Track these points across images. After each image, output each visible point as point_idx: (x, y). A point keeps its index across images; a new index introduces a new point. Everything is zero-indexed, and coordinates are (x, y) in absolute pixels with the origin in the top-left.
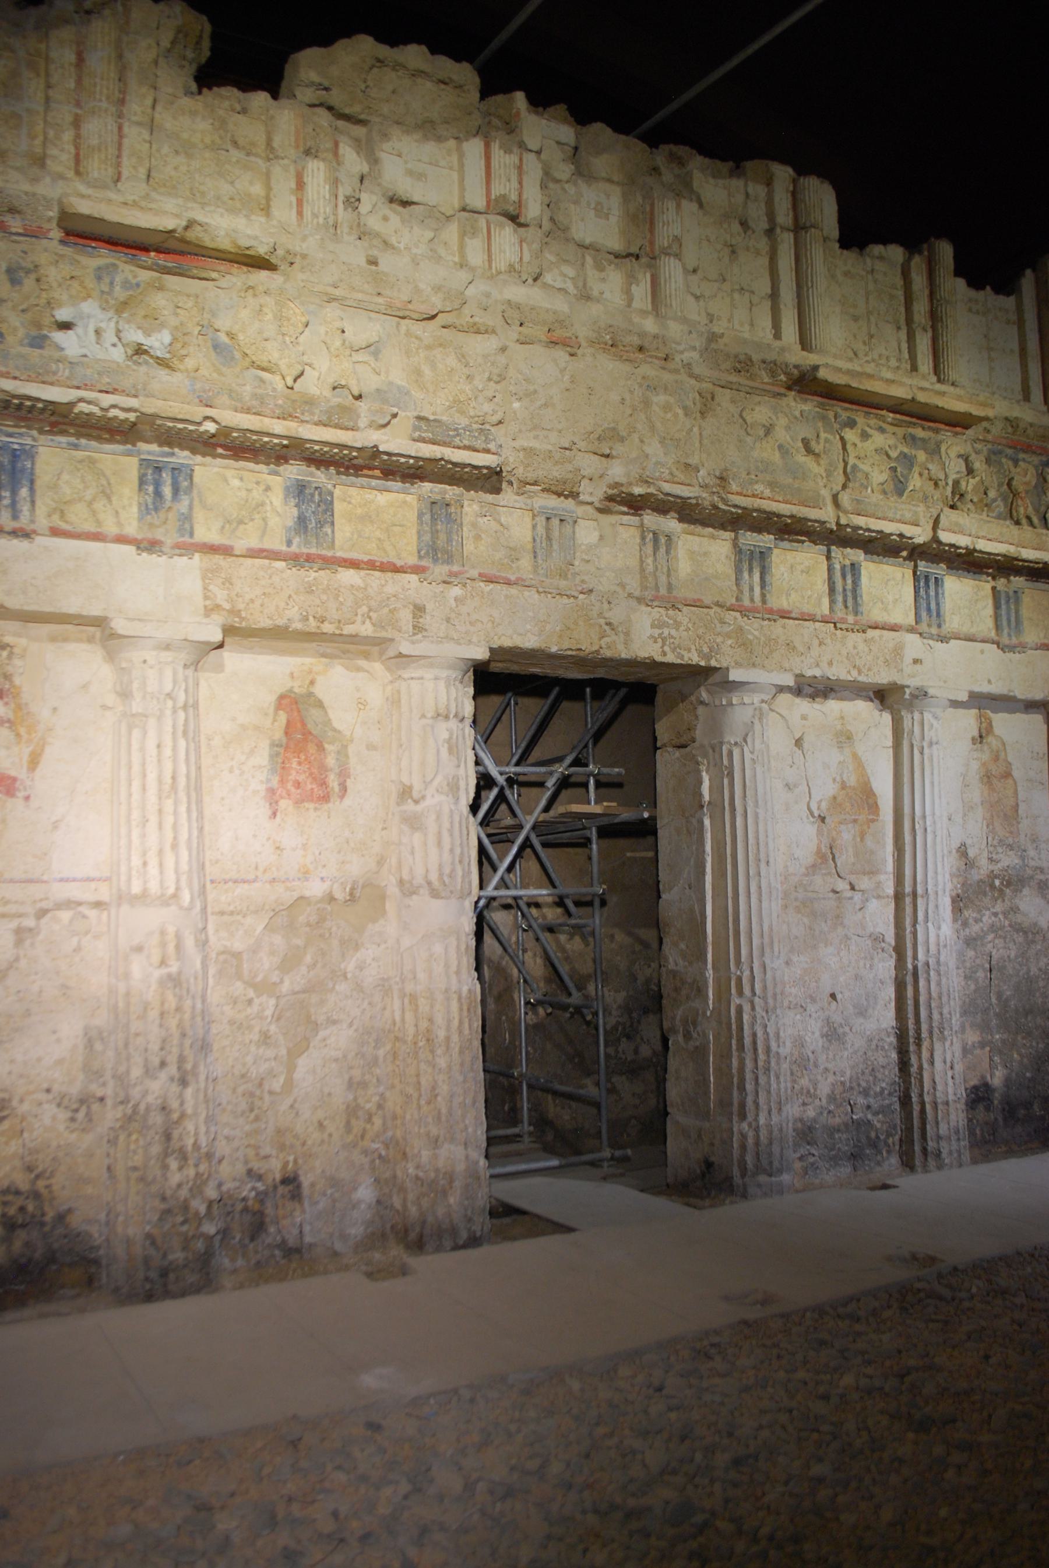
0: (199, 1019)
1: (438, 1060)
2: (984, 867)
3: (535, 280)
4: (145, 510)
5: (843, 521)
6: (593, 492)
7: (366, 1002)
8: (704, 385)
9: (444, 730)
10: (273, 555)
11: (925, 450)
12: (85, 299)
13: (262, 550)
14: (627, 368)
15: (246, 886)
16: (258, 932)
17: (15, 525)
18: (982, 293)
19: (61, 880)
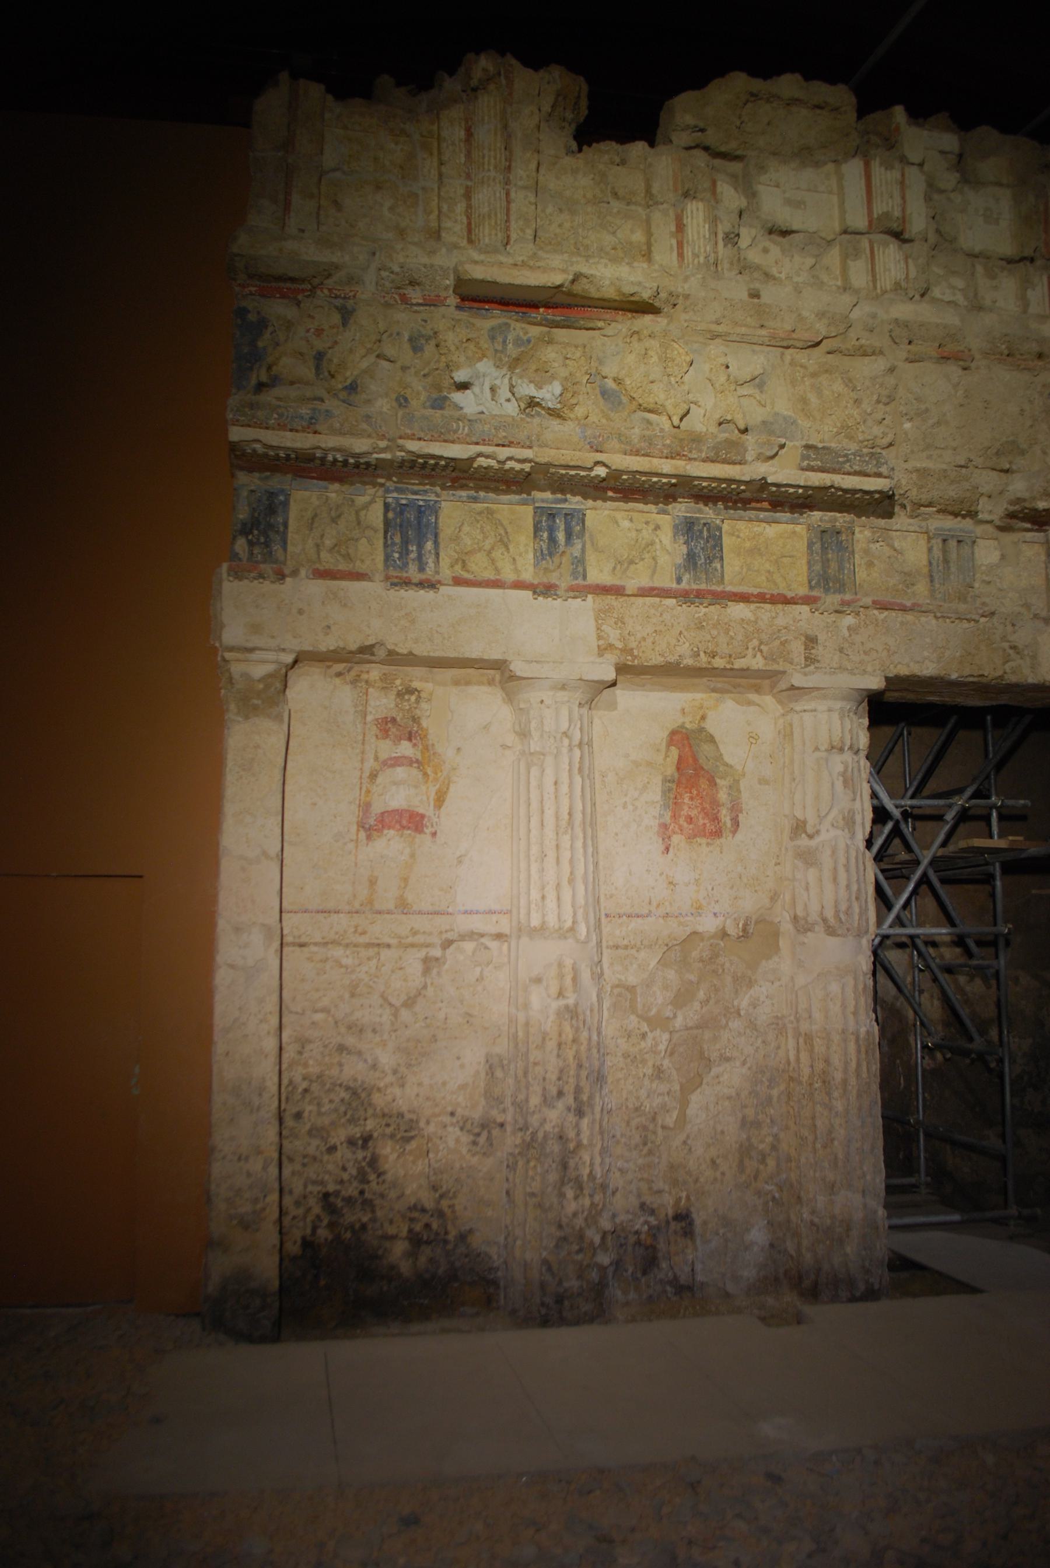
0: (594, 1051)
1: (834, 1102)
3: (922, 295)
4: (540, 556)
6: (992, 510)
7: (760, 1041)
9: (838, 762)
12: (480, 359)
13: (653, 589)
15: (640, 920)
16: (651, 966)
17: (423, 577)
19: (465, 912)
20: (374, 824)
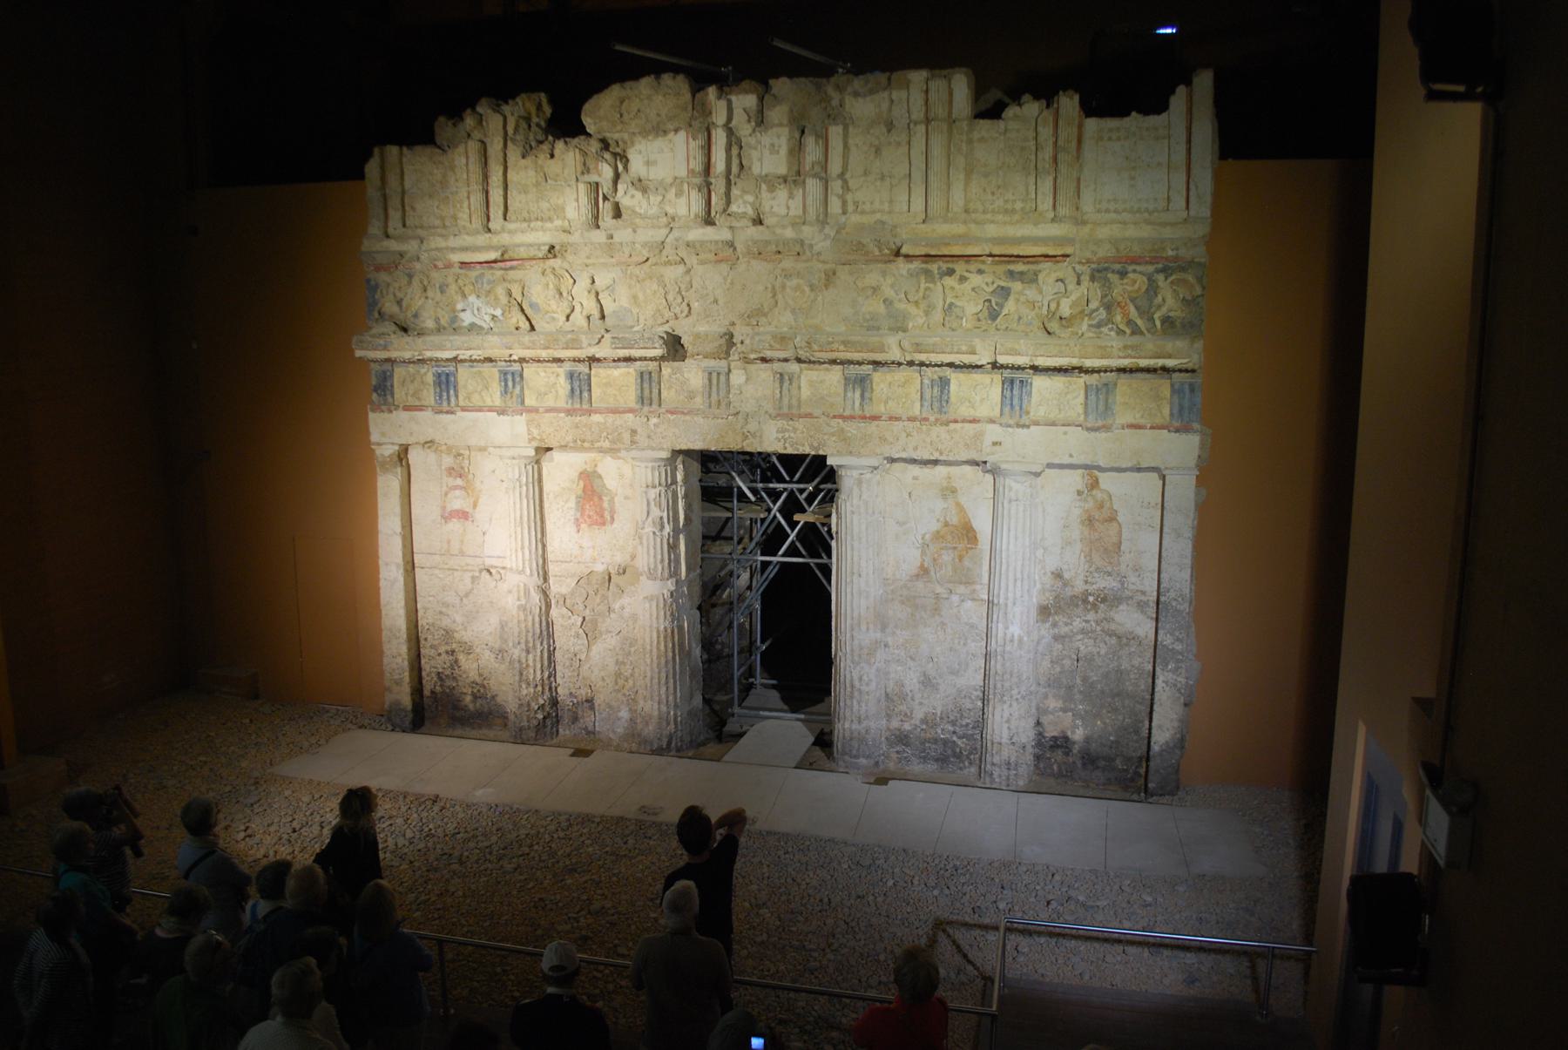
2: (1079, 587)
8: (828, 266)
9: (653, 493)
20: (448, 516)
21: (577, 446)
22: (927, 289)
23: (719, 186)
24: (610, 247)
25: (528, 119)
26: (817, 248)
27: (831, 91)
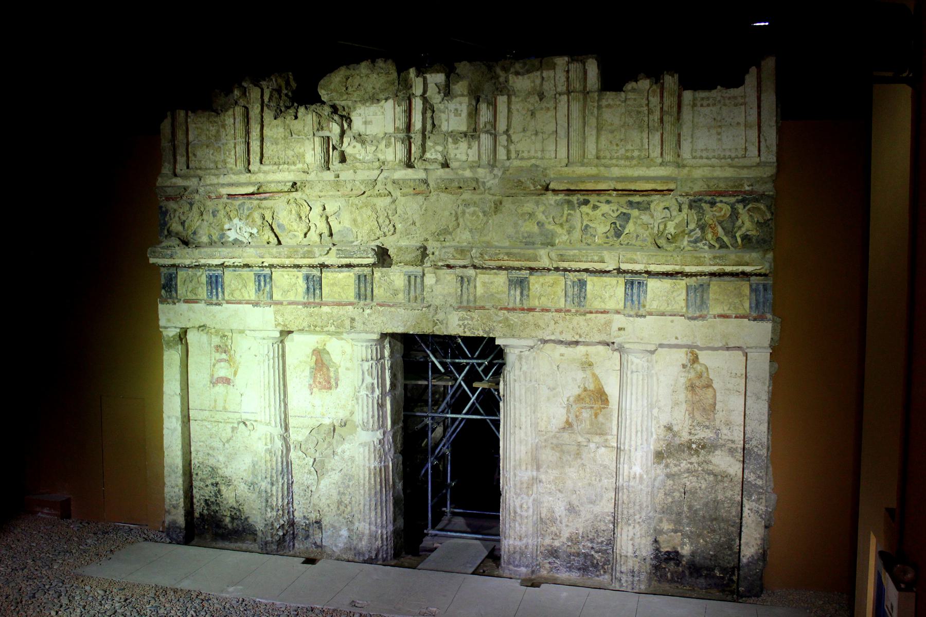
0: (280, 464)
2: (685, 437)
5: (555, 266)
9: (366, 365)
10: (297, 303)
11: (639, 210)
14: (454, 197)
18: (714, 91)
20: (215, 381)
21: (312, 329)
22: (569, 214)
23: (417, 139)
24: (337, 183)
25: (279, 91)
26: (488, 185)
27: (498, 71)
